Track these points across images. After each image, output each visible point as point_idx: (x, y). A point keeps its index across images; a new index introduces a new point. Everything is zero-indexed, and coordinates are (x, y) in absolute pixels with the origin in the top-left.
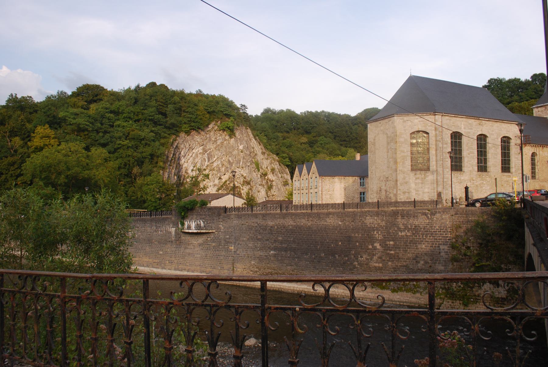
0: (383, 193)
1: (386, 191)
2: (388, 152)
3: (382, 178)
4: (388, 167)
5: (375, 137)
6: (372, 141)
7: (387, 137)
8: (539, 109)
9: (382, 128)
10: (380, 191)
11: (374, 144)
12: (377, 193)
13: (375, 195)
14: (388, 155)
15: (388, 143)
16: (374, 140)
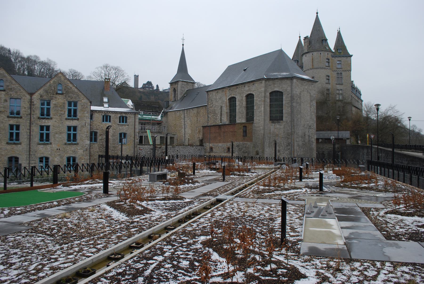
0: (307, 137)
1: (309, 136)
2: (311, 107)
3: (306, 126)
4: (310, 118)
5: (301, 92)
6: (299, 94)
7: (310, 96)
8: (183, 83)
9: (306, 87)
10: (305, 135)
11: (300, 97)
12: (302, 137)
13: (300, 139)
14: (310, 109)
15: (311, 101)
16: (300, 94)
